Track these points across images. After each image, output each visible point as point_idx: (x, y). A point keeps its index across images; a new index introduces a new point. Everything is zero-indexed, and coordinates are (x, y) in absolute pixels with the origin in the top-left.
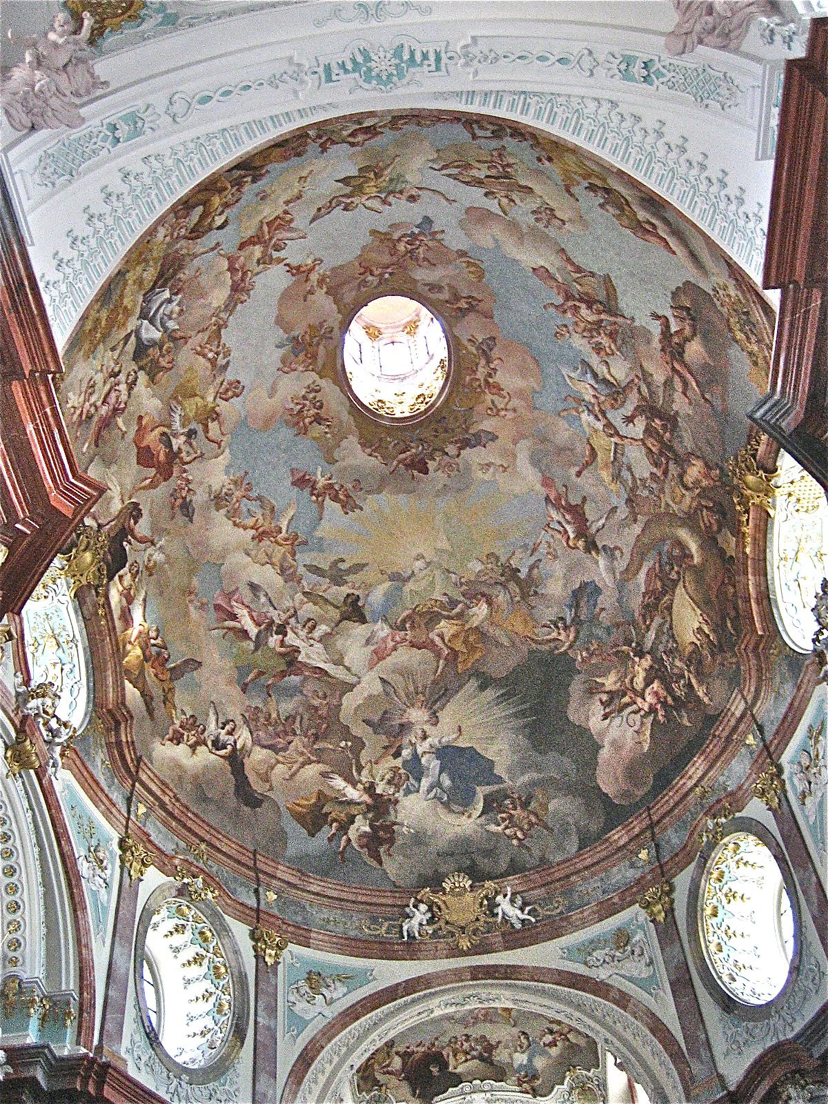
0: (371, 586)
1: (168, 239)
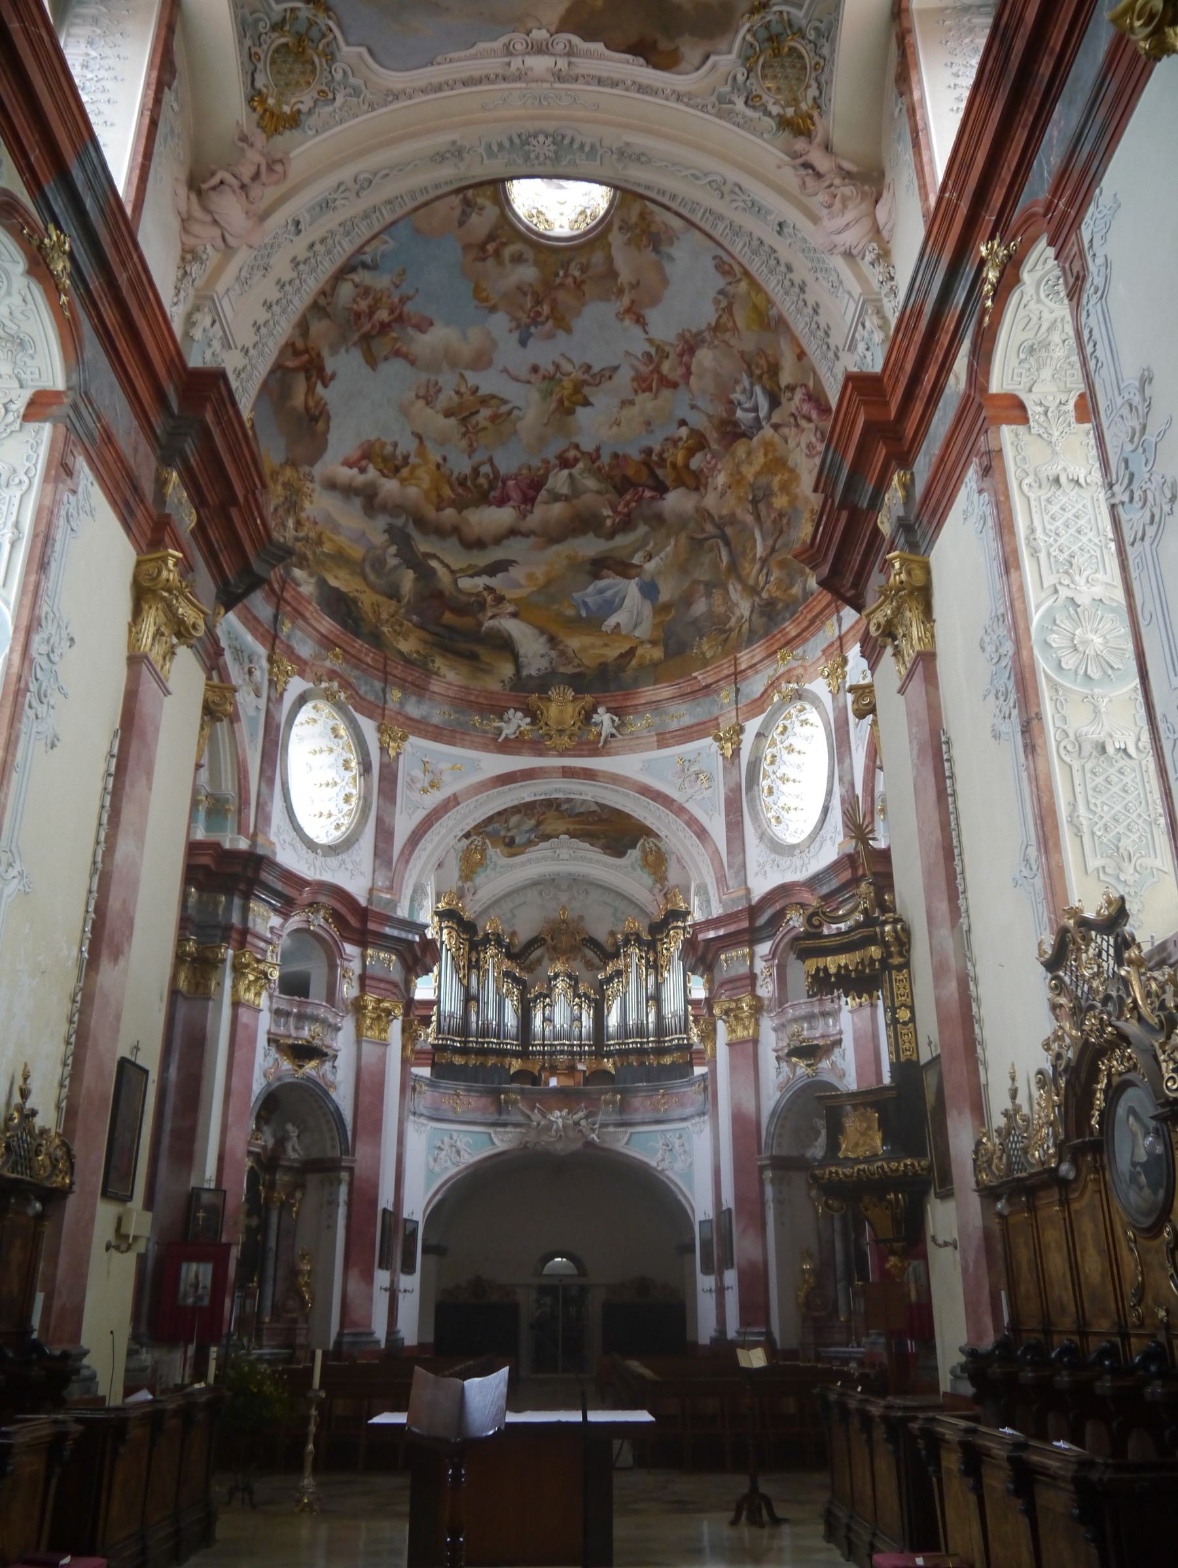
1: (719, 466)
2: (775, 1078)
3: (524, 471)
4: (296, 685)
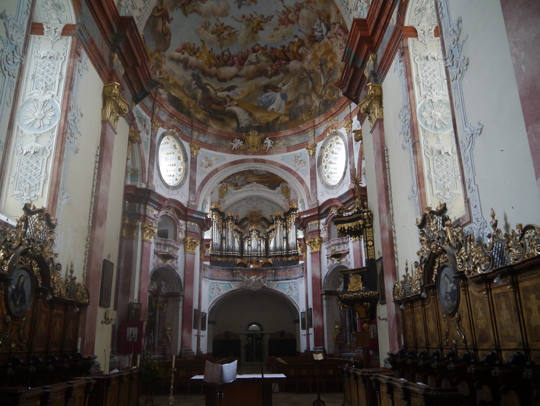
2: (327, 265)
3: (240, 54)
4: (161, 130)
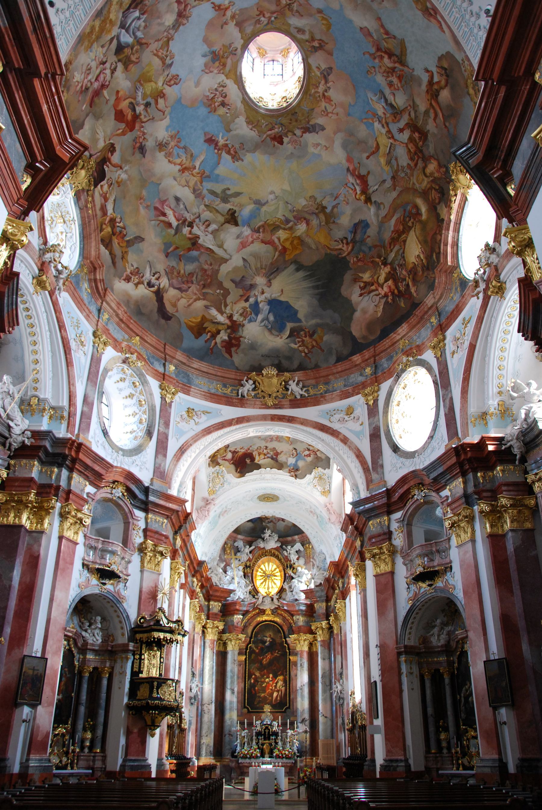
0: (243, 205)
